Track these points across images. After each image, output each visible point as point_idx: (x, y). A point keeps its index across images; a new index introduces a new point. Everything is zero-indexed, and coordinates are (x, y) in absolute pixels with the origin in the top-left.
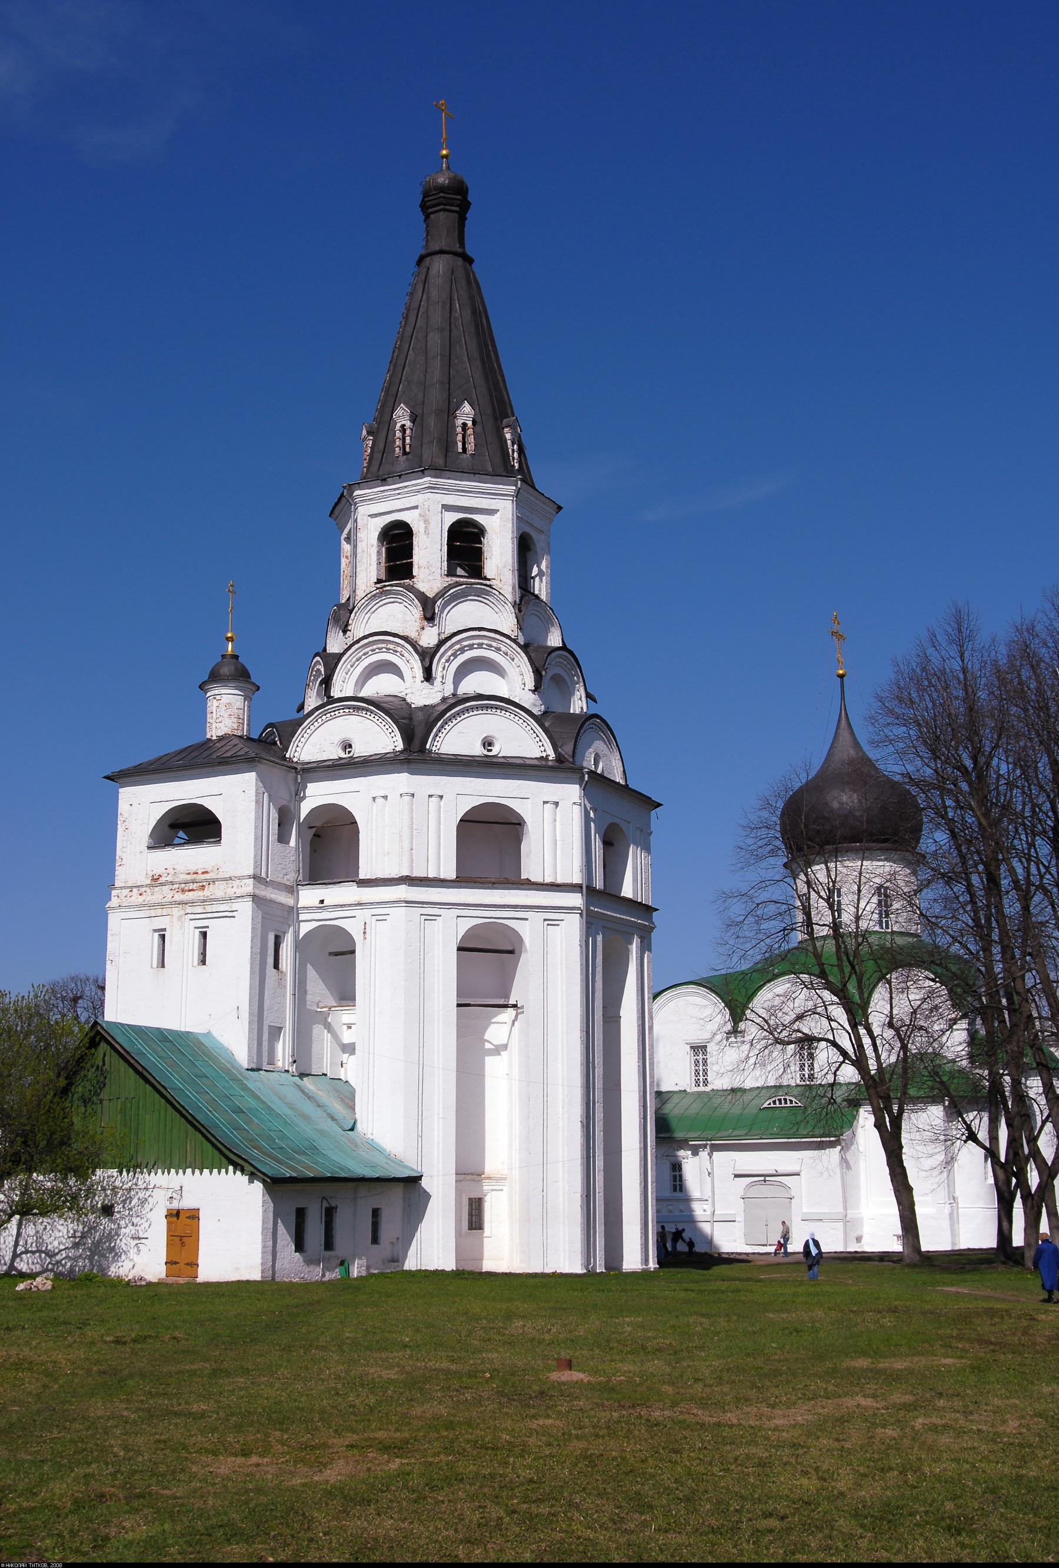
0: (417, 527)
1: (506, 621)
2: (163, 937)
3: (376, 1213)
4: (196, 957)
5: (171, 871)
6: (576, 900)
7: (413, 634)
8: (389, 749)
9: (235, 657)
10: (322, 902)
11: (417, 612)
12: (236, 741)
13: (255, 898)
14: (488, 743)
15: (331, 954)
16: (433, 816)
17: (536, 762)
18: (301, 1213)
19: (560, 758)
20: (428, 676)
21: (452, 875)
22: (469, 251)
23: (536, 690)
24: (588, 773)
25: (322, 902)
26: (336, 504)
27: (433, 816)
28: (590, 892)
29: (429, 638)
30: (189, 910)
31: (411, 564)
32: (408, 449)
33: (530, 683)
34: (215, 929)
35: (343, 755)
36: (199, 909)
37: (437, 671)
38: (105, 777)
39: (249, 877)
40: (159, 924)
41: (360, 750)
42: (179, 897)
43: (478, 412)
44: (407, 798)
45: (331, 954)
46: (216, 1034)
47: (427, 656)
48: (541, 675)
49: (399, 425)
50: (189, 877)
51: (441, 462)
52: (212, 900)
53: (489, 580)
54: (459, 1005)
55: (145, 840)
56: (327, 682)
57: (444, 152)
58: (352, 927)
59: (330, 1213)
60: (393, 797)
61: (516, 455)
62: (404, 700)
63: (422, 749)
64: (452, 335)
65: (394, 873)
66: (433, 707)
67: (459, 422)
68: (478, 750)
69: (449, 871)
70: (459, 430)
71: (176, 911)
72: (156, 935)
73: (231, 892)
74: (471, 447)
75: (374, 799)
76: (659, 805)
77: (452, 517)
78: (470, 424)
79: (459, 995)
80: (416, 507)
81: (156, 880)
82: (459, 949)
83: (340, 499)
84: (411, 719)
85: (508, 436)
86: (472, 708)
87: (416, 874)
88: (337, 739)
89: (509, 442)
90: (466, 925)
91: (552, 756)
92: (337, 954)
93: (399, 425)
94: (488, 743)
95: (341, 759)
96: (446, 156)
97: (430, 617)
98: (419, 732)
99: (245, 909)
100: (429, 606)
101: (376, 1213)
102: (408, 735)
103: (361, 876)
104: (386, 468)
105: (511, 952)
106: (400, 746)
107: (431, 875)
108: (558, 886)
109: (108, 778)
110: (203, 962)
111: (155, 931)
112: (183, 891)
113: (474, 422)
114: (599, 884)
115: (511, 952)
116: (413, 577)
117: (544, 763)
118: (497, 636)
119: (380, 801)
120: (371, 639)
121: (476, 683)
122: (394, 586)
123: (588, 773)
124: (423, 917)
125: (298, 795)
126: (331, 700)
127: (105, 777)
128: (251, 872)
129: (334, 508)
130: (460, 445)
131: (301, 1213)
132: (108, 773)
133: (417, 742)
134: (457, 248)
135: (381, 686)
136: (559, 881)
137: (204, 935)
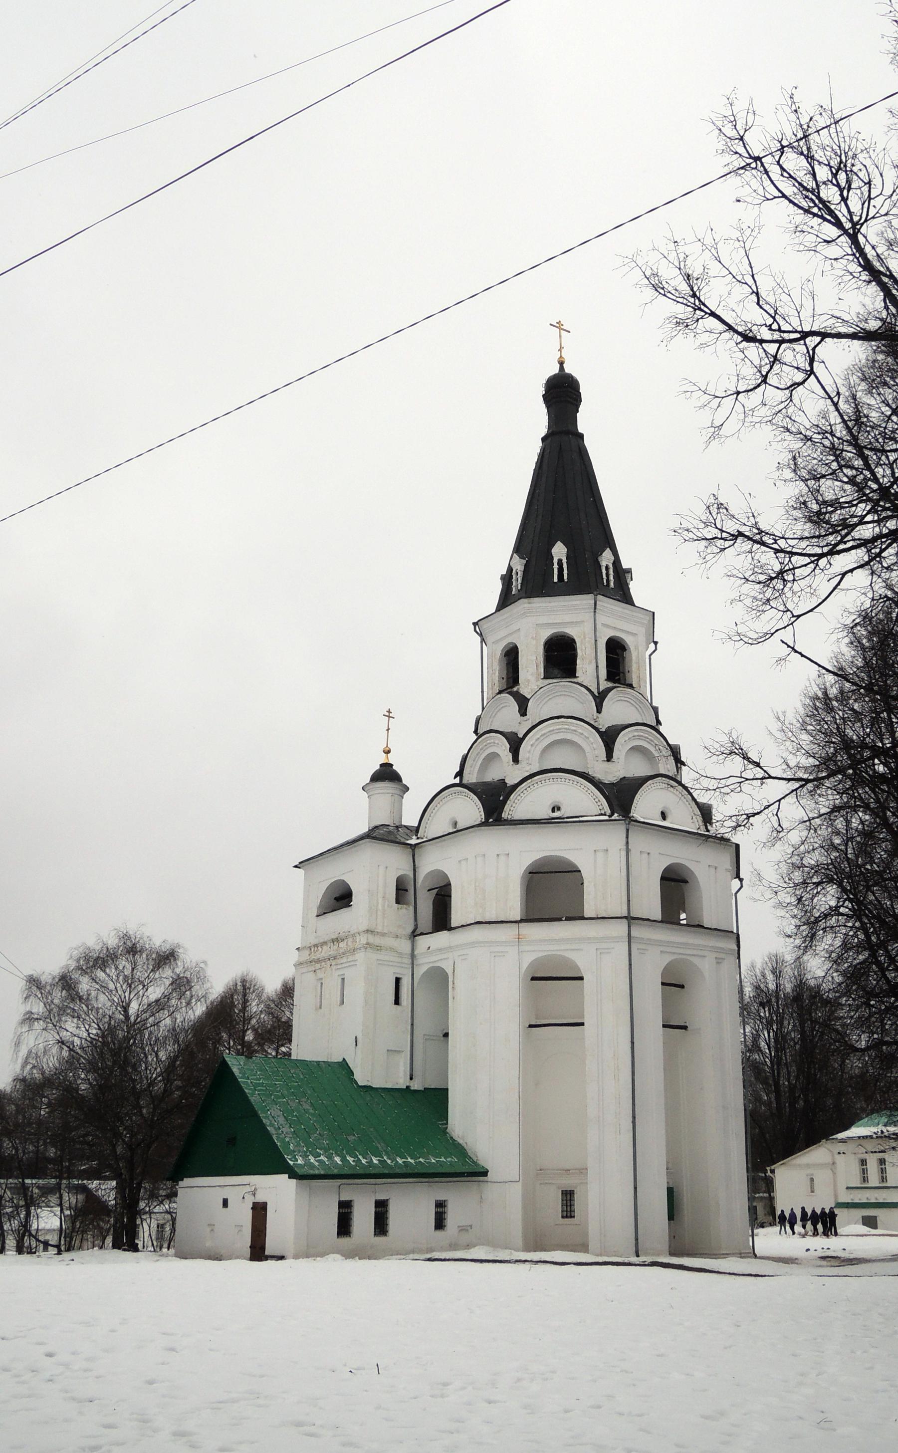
3: (441, 1205)
4: (339, 999)
20: (516, 760)
34: (348, 973)
40: (341, 972)
49: (514, 572)
68: (546, 813)
77: (546, 634)
78: (564, 561)
90: (528, 959)
97: (523, 712)
101: (441, 1205)
109: (296, 867)
110: (342, 1003)
119: (464, 863)
124: (493, 955)
137: (343, 979)
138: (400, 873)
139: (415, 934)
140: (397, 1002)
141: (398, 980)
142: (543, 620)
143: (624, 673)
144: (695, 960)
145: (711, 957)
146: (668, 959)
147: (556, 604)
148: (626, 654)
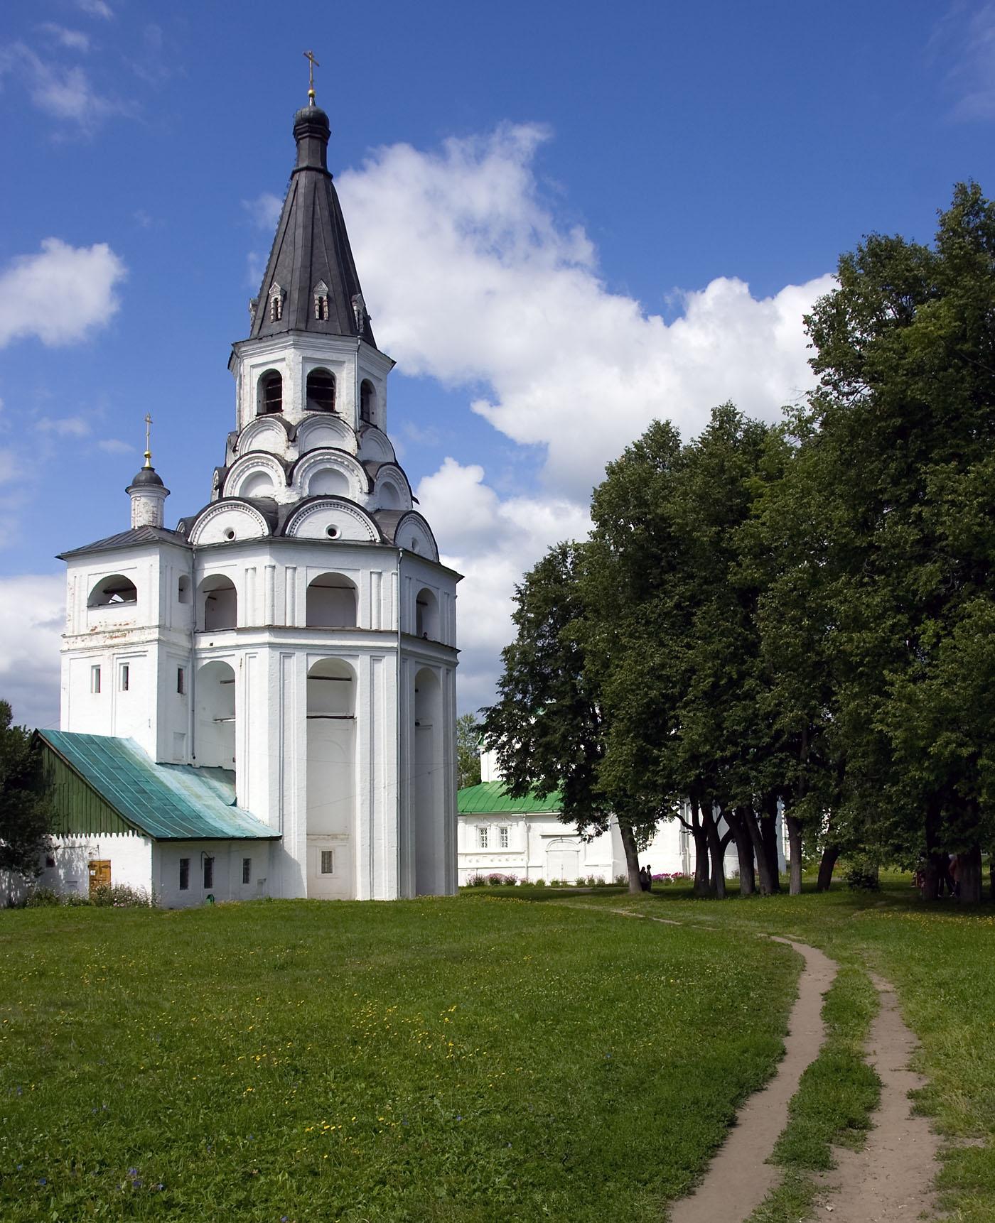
0: (285, 374)
1: (350, 444)
2: (99, 671)
5: (104, 624)
6: (394, 644)
7: (281, 452)
8: (259, 535)
9: (151, 469)
10: (212, 644)
11: (283, 435)
12: (150, 530)
13: (159, 640)
14: (332, 532)
15: (221, 682)
16: (289, 582)
17: (367, 544)
18: (185, 864)
19: (383, 541)
21: (304, 625)
22: (329, 170)
23: (370, 492)
24: (402, 551)
25: (212, 644)
26: (231, 359)
27: (289, 582)
28: (404, 637)
29: (292, 456)
30: (116, 651)
31: (280, 402)
32: (279, 317)
33: (366, 489)
34: (134, 664)
35: (228, 540)
36: (122, 651)
37: (298, 479)
38: (57, 557)
39: (156, 627)
40: (95, 662)
41: (239, 536)
42: (109, 642)
43: (332, 290)
44: (269, 570)
45: (221, 682)
46: (136, 739)
47: (289, 468)
48: (373, 482)
50: (115, 628)
51: (302, 326)
52: (132, 644)
53: (338, 413)
54: (308, 717)
55: (85, 603)
56: (220, 487)
57: (310, 92)
58: (233, 662)
59: (208, 864)
60: (260, 570)
61: (361, 322)
62: (274, 500)
63: (283, 534)
64: (315, 231)
65: (261, 622)
66: (293, 504)
67: (316, 296)
68: (324, 535)
69: (301, 621)
70: (317, 302)
71: (107, 652)
72: (94, 671)
73: (143, 638)
74: (326, 315)
75: (247, 570)
76: (463, 577)
78: (325, 298)
79: (308, 710)
80: (283, 360)
81: (94, 632)
82: (310, 677)
83: (232, 355)
84: (277, 513)
85: (355, 308)
86: (320, 505)
87: (277, 623)
88: (223, 528)
89: (356, 313)
90: (313, 660)
91: (378, 540)
92: (226, 682)
93: (273, 299)
94: (332, 532)
95: (226, 542)
96: (312, 95)
98: (281, 524)
99: (153, 650)
100: (293, 432)
102: (273, 524)
103: (239, 626)
104: (265, 331)
105: (349, 680)
106: (267, 533)
107: (288, 625)
108: (381, 632)
110: (127, 689)
111: (93, 667)
112: (111, 637)
113: (328, 296)
114: (412, 630)
115: (349, 680)
116: (282, 411)
117: (373, 544)
118: (341, 453)
120: (250, 456)
121: (326, 488)
122: (269, 418)
123: (402, 551)
125: (195, 568)
126: (221, 499)
127: (57, 557)
128: (157, 624)
129: (230, 362)
130: (317, 313)
131: (185, 864)
132: (59, 554)
133: (278, 531)
134: (319, 165)
135: (259, 491)
136: (382, 629)
138: (184, 574)
139: (193, 634)
140: (180, 690)
141: (180, 670)
142: (309, 354)
143: (368, 414)
144: (434, 670)
145: (444, 668)
146: (420, 667)
147: (322, 341)
148: (371, 396)
